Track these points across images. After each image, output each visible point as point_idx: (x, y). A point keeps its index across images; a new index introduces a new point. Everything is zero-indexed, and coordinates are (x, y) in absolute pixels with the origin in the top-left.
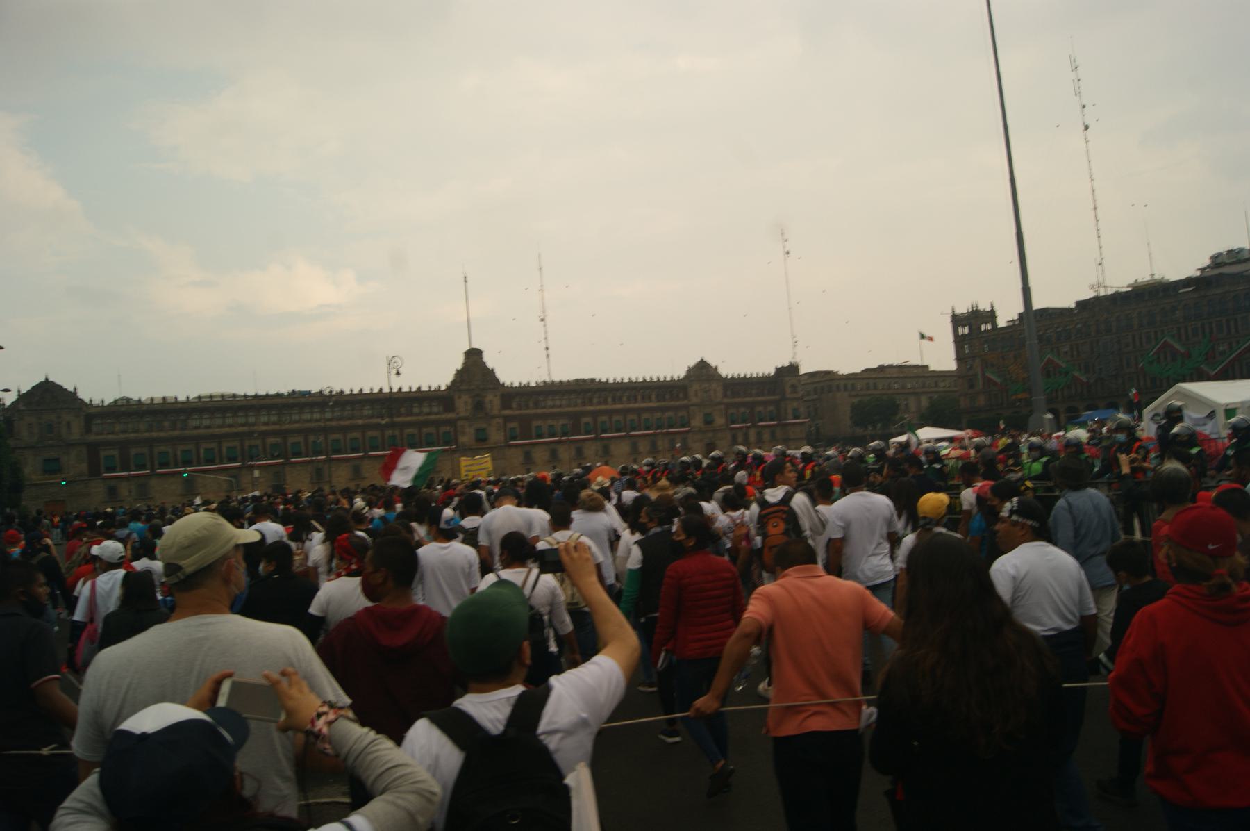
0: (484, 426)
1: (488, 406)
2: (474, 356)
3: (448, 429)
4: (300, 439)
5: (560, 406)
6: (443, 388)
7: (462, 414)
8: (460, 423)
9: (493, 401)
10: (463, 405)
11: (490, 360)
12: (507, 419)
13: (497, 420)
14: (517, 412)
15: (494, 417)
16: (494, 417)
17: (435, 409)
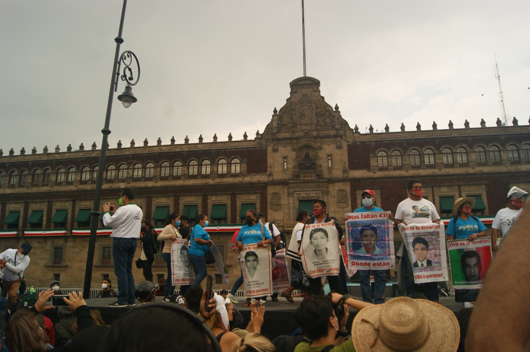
0: (313, 195)
1: (324, 164)
2: (305, 88)
3: (253, 198)
4: (20, 207)
5: (466, 165)
6: (252, 137)
7: (277, 176)
8: (271, 190)
9: (333, 159)
10: (281, 163)
11: (331, 94)
12: (357, 184)
13: (339, 186)
14: (379, 174)
15: (331, 181)
16: (331, 181)
17: (236, 168)
